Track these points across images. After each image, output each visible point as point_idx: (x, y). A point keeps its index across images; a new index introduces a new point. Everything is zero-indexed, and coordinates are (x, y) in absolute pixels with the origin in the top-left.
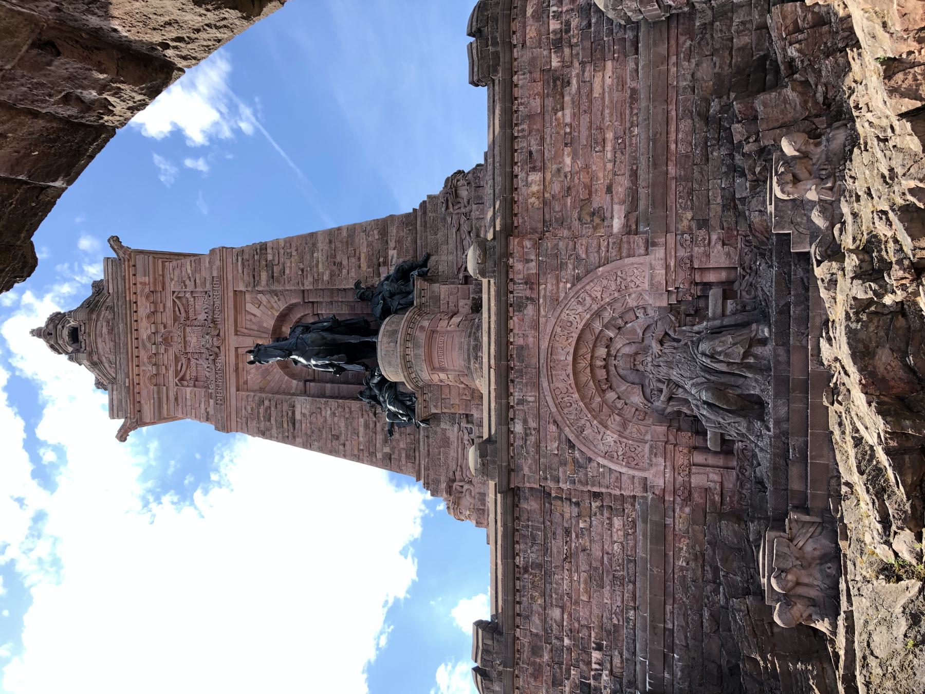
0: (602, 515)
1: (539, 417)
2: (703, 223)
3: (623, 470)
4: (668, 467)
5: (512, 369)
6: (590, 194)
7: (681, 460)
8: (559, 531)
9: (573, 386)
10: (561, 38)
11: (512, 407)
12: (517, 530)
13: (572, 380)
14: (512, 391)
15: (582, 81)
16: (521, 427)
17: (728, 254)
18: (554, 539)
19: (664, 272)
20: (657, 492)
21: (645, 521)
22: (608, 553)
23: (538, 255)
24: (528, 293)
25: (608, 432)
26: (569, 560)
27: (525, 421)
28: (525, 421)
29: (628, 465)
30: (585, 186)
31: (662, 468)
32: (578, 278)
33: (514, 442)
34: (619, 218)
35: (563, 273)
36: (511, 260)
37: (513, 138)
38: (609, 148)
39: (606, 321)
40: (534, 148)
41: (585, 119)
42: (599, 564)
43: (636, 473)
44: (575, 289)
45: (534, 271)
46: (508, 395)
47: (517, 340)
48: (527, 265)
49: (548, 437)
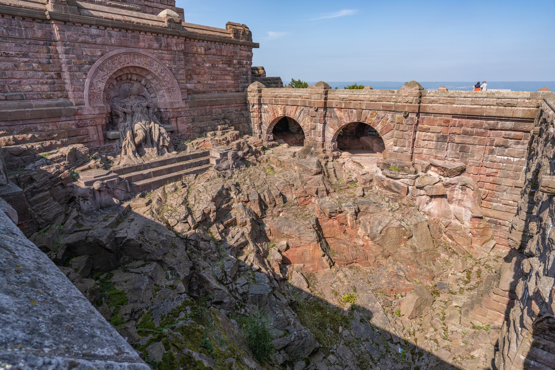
0: (48, 78)
1: (103, 44)
2: (193, 120)
3: (86, 93)
4: (94, 116)
5: (127, 31)
6: (197, 74)
7: (98, 121)
8: (25, 50)
9: (124, 66)
10: (241, 64)
11: (106, 28)
12: (13, 17)
13: (126, 65)
14: (115, 30)
15: (229, 71)
16: (95, 33)
17: (185, 130)
18: (16, 45)
19: (177, 107)
20: (79, 111)
21: (57, 105)
22: (20, 82)
23: (179, 51)
24: (163, 45)
25: (104, 84)
26: (4, 55)
27: (99, 36)
28: (99, 36)
29: (89, 95)
30: (200, 72)
31: (94, 113)
32: (171, 70)
33: (85, 27)
34: (190, 86)
35: (172, 63)
36: (176, 37)
37: (215, 42)
38: (211, 82)
39: (151, 81)
40: (213, 51)
41: (218, 72)
42: (10, 76)
43: (86, 100)
44: (168, 69)
45: (172, 49)
46: (113, 28)
47: (142, 36)
48: (174, 45)
49: (92, 49)
